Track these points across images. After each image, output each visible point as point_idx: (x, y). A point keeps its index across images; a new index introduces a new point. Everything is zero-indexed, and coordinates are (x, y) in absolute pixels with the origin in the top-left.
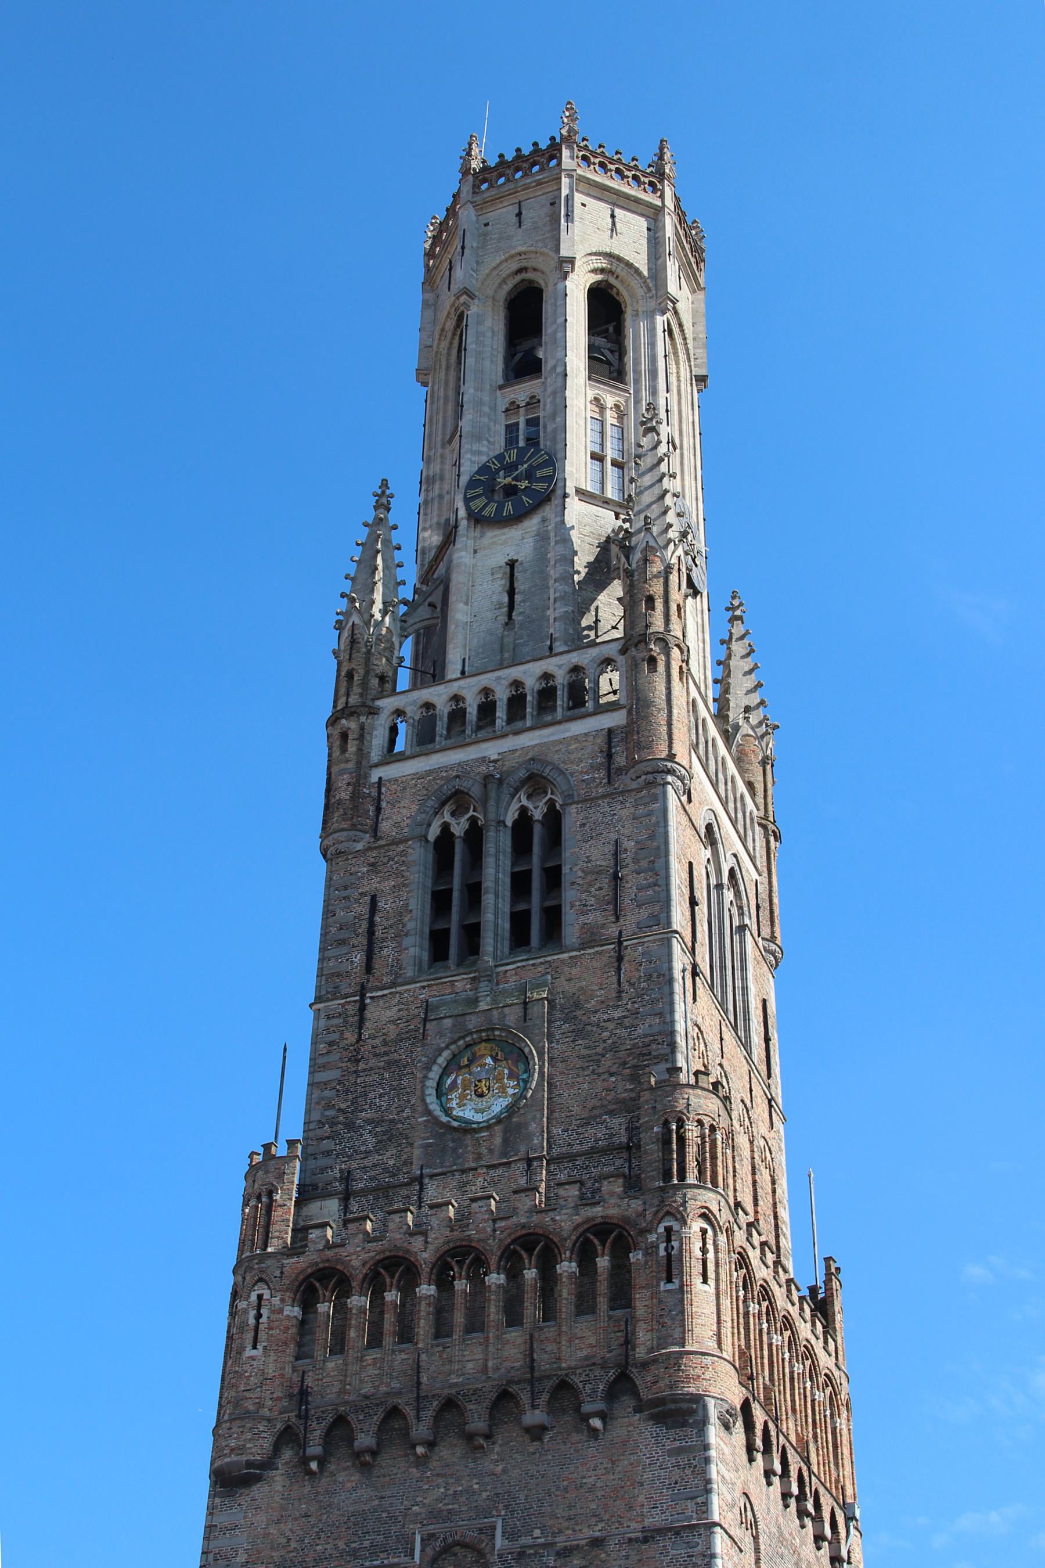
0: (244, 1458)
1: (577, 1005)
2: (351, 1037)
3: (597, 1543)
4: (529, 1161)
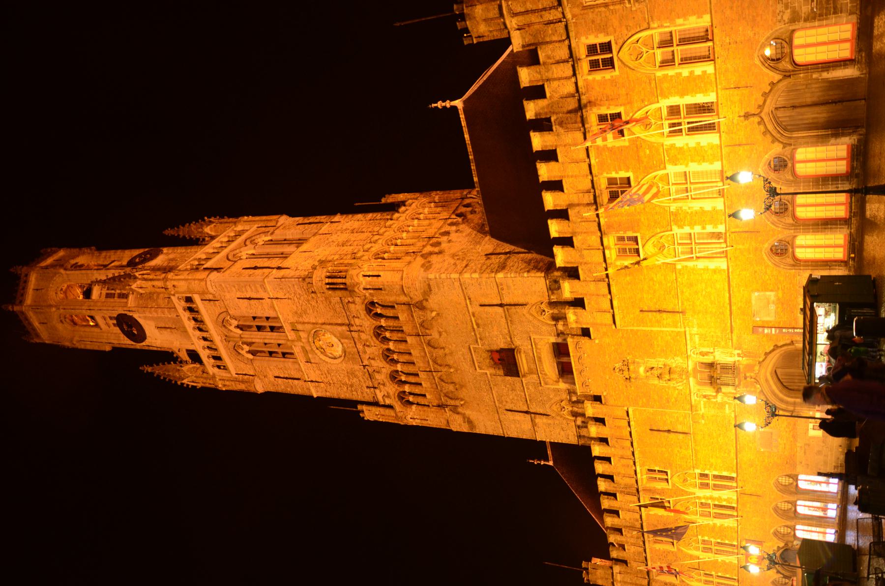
1: (296, 313)
2: (322, 385)
4: (351, 331)
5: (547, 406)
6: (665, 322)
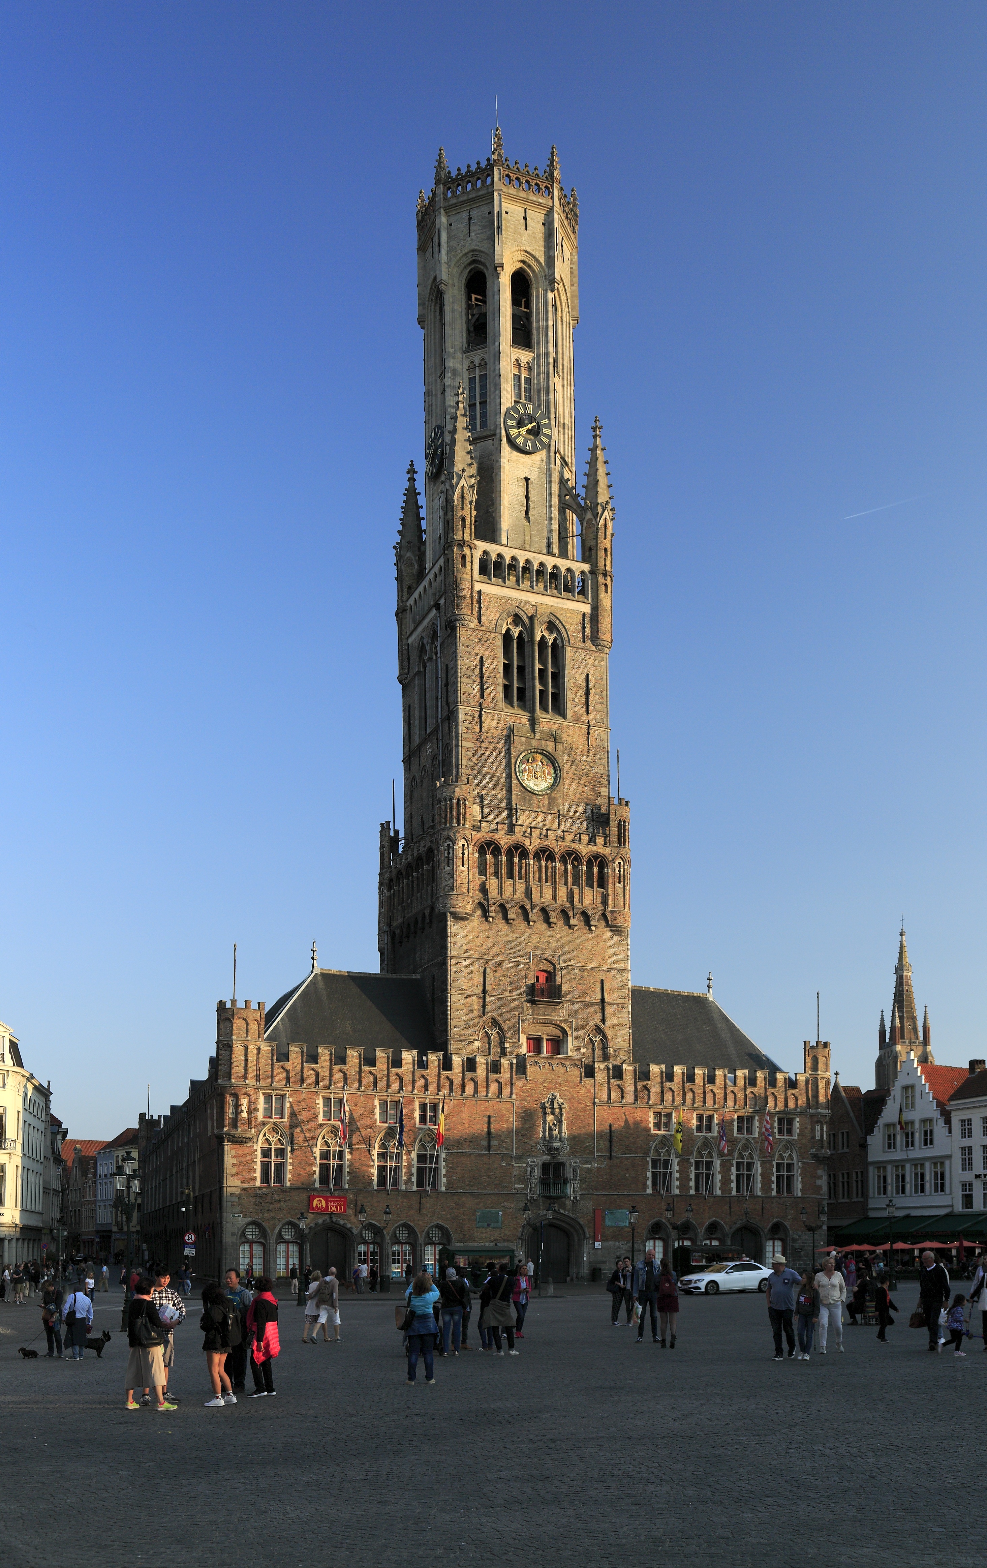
0: (465, 911)
2: (478, 730)
3: (592, 969)
5: (496, 1016)
6: (601, 1142)
